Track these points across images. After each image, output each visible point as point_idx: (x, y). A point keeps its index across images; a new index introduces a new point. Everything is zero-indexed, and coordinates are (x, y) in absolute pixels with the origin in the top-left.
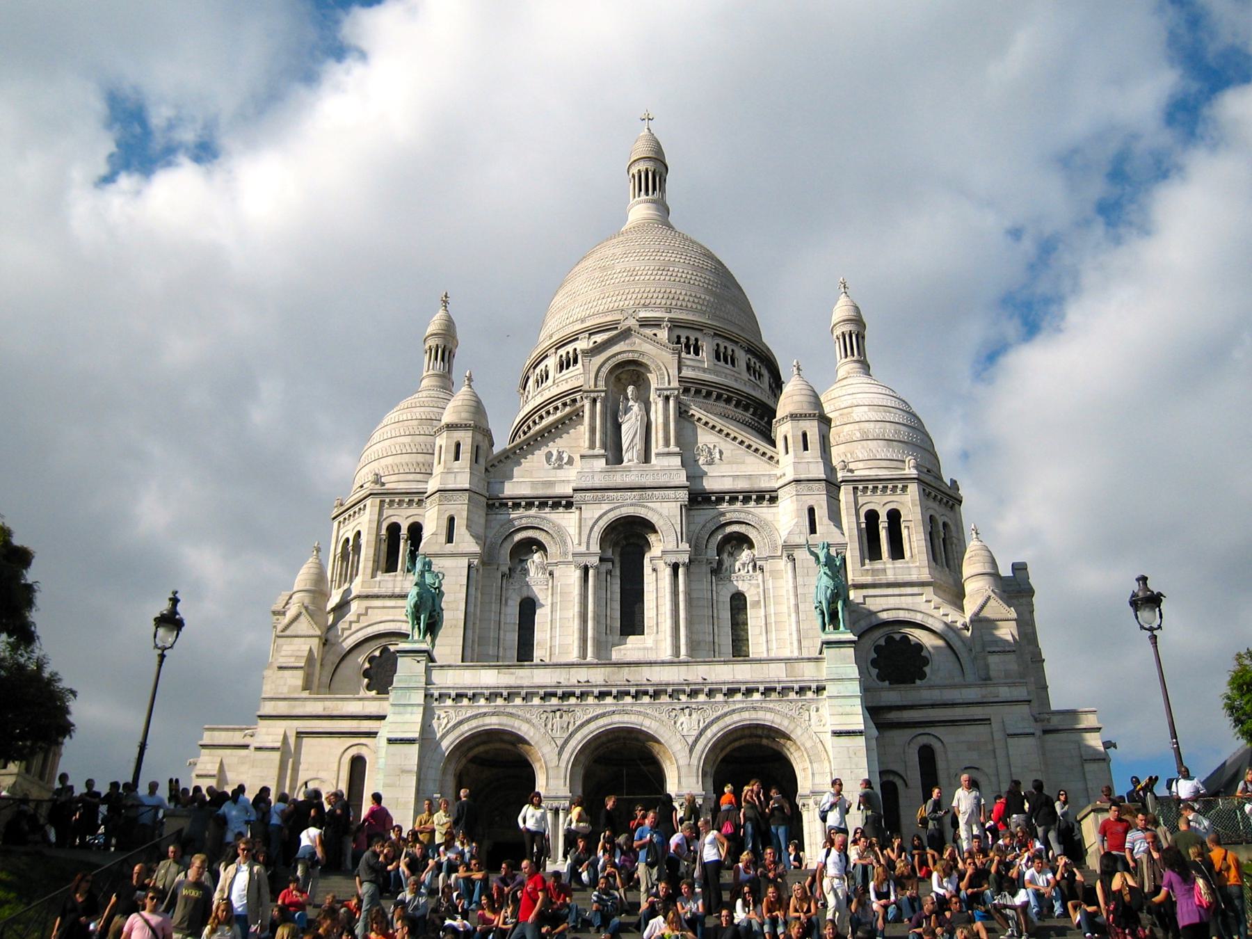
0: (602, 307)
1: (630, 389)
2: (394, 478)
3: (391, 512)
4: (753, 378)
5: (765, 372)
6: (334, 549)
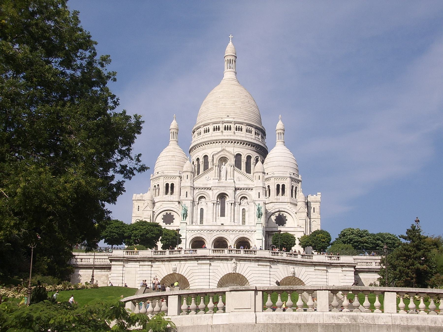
0: (216, 115)
1: (224, 163)
2: (166, 172)
3: (166, 180)
4: (256, 136)
5: (260, 133)
6: (152, 187)
